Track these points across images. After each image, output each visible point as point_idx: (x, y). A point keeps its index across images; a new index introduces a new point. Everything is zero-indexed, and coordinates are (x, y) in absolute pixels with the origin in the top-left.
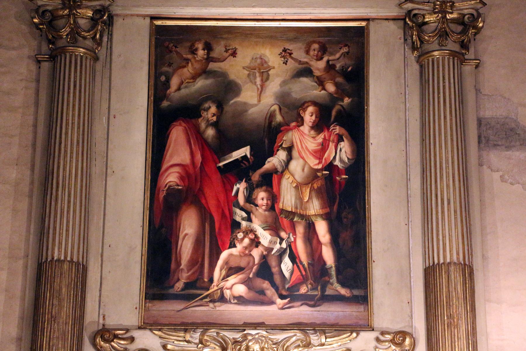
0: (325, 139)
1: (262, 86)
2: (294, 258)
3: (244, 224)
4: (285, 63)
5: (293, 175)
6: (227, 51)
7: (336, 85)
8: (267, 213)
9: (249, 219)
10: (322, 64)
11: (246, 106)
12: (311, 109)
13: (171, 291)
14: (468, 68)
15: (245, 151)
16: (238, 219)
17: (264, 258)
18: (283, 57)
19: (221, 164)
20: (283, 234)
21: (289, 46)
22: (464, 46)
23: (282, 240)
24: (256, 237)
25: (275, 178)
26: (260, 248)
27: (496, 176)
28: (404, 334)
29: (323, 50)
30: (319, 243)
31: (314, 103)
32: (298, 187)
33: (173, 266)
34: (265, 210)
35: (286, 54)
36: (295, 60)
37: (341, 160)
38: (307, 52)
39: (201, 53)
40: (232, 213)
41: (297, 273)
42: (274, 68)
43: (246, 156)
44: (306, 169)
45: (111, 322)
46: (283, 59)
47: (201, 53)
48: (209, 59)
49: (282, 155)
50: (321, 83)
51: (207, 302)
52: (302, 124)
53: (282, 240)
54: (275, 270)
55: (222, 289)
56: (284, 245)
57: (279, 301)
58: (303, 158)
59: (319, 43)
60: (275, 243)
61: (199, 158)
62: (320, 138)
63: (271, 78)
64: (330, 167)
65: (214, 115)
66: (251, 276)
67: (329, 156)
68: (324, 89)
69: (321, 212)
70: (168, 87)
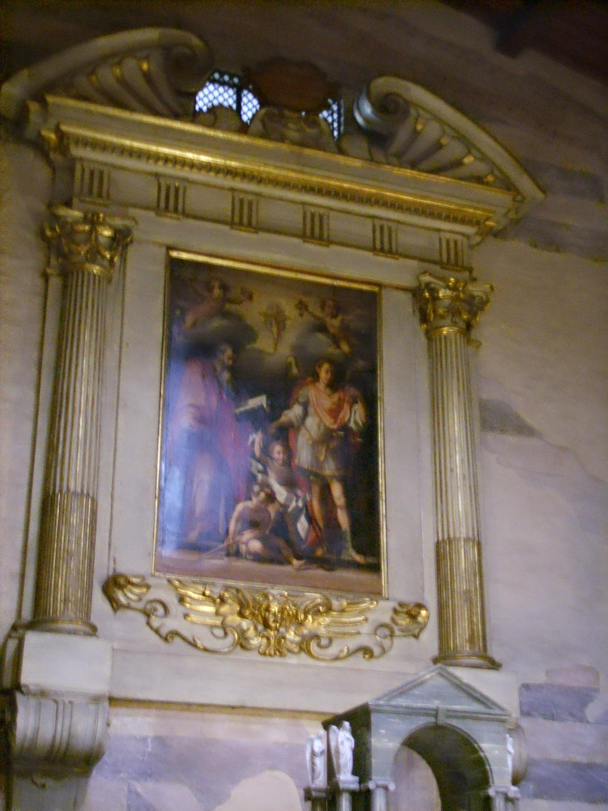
0: (340, 399)
1: (279, 334)
2: (311, 519)
3: (260, 477)
7: (351, 346)
8: (283, 468)
9: (265, 472)
10: (336, 322)
12: (326, 366)
16: (254, 471)
18: (301, 309)
20: (299, 492)
21: (306, 299)
26: (276, 505)
32: (315, 444)
35: (302, 307)
36: (311, 314)
37: (355, 422)
38: (323, 307)
39: (217, 292)
41: (313, 535)
42: (290, 318)
43: (262, 406)
44: (322, 428)
45: (124, 567)
47: (217, 292)
49: (297, 410)
50: (336, 342)
53: (298, 497)
56: (300, 504)
57: (295, 562)
58: (319, 416)
59: (334, 301)
60: (291, 501)
62: (336, 397)
64: (345, 427)
66: (267, 532)
67: (344, 417)
68: (338, 347)
69: (336, 473)
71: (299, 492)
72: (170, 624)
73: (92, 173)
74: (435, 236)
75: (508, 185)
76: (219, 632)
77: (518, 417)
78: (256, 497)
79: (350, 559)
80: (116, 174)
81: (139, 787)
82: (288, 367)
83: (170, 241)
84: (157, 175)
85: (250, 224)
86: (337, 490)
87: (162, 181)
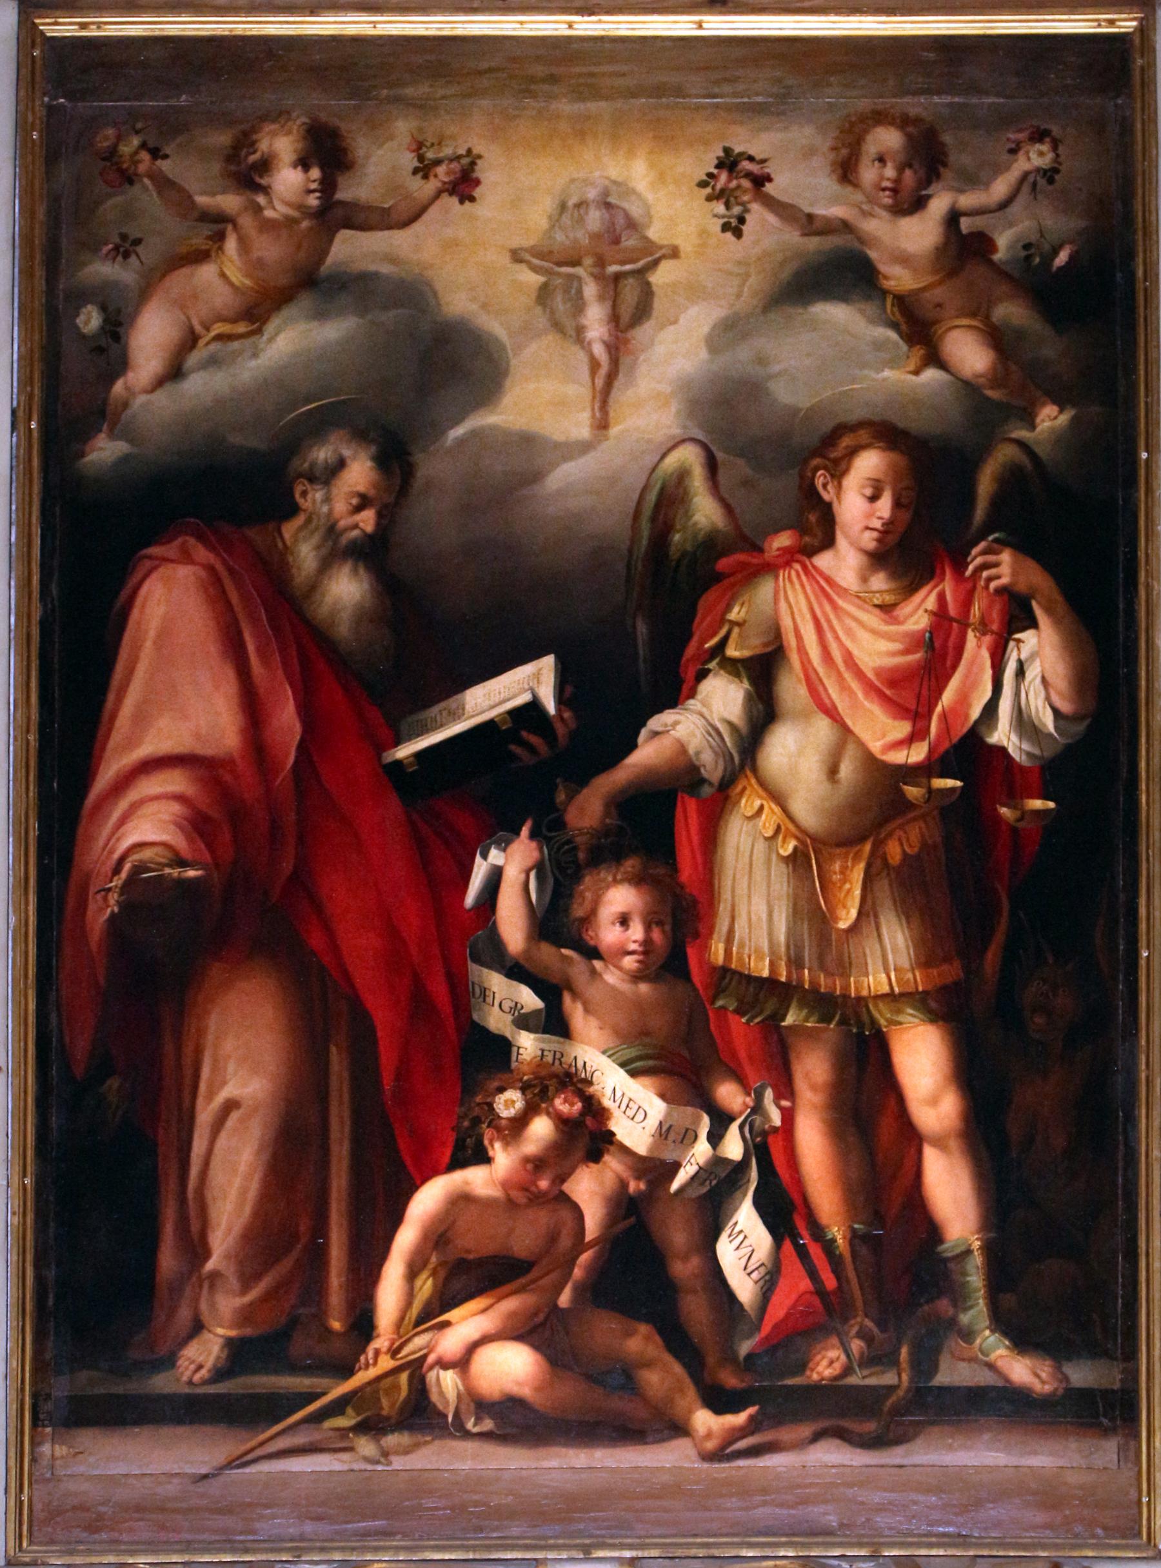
0: (940, 615)
1: (617, 348)
3: (528, 1044)
4: (735, 228)
5: (778, 798)
6: (424, 170)
8: (644, 988)
13: (161, 1383)
16: (497, 1021)
19: (404, 751)
20: (729, 1094)
23: (721, 1121)
24: (595, 1111)
26: (613, 1164)
33: (168, 1260)
34: (636, 977)
37: (1023, 723)
38: (846, 171)
42: (674, 253)
43: (534, 706)
44: (847, 770)
46: (720, 208)
51: (343, 1432)
52: (828, 542)
53: (721, 1121)
54: (684, 1269)
55: (417, 1368)
56: (733, 1148)
57: (704, 1420)
58: (831, 712)
60: (688, 1137)
63: (658, 304)
65: (364, 502)
66: (565, 1299)
67: (964, 699)
68: (934, 358)
69: (918, 980)
70: (121, 364)
71: (729, 1094)
78: (506, 1144)
79: (984, 1378)
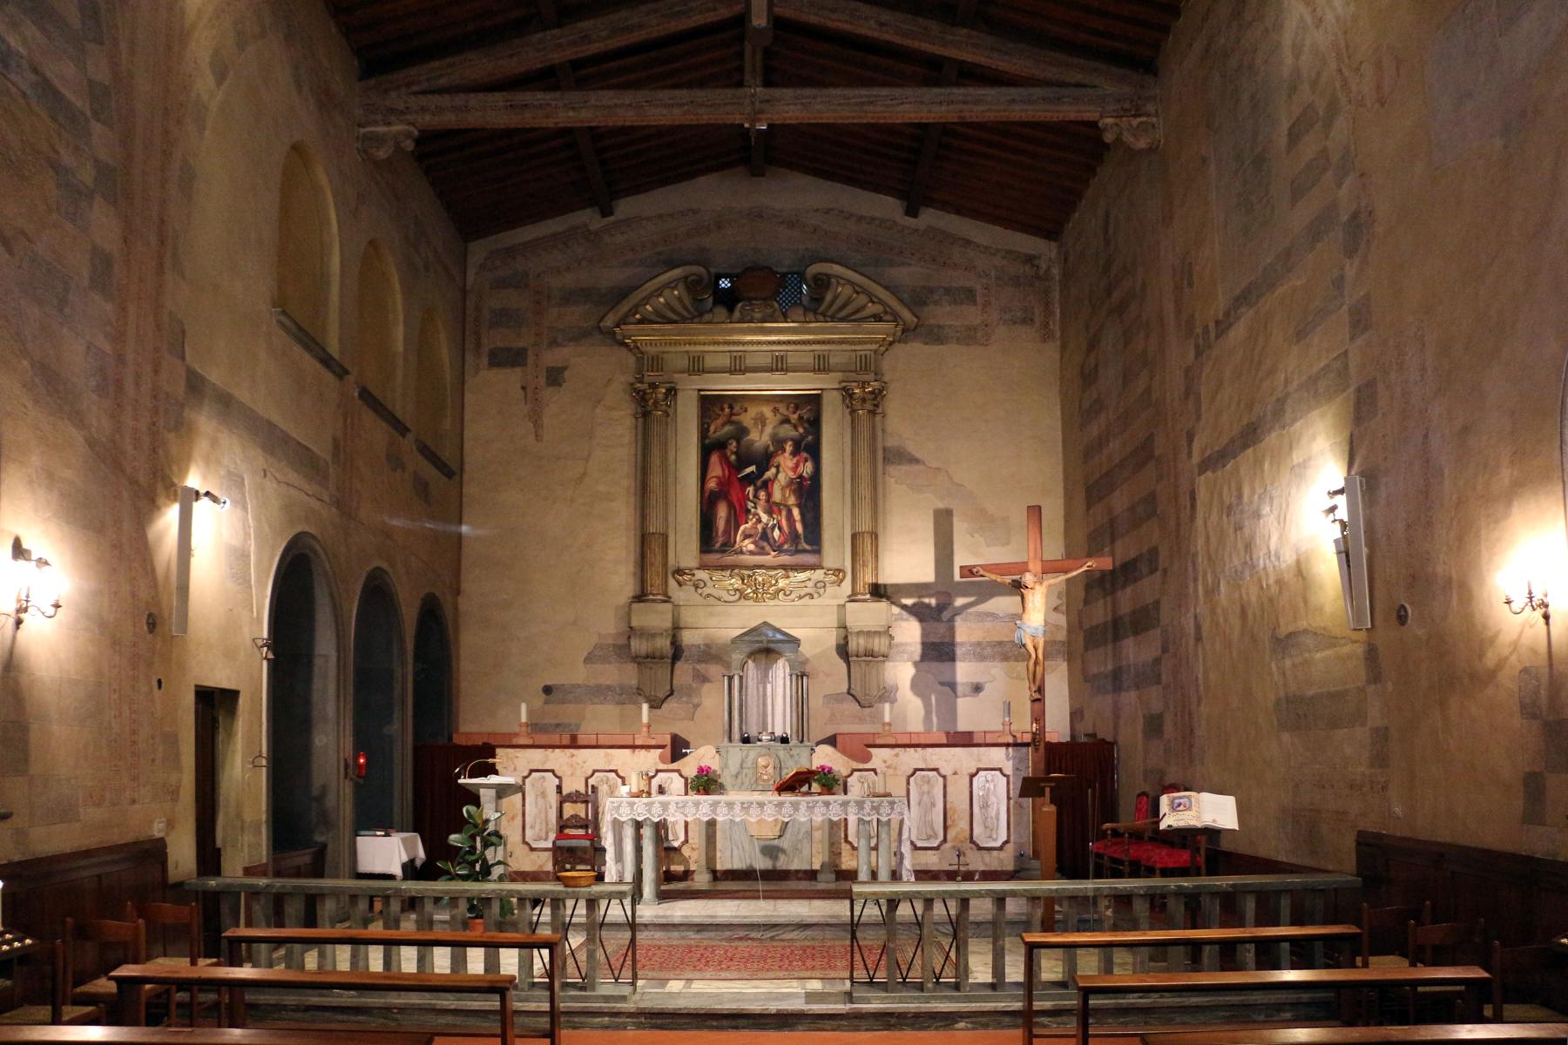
2: (780, 529)
3: (753, 510)
7: (804, 428)
9: (756, 508)
10: (796, 416)
11: (752, 442)
12: (790, 443)
14: (878, 418)
15: (752, 468)
17: (764, 529)
20: (775, 516)
22: (876, 406)
25: (770, 484)
27: (893, 480)
28: (839, 570)
29: (797, 408)
30: (795, 521)
31: (792, 440)
32: (783, 489)
33: (714, 534)
35: (775, 410)
38: (788, 409)
39: (727, 410)
40: (746, 505)
41: (782, 538)
45: (683, 565)
47: (727, 410)
48: (732, 414)
49: (773, 470)
50: (795, 427)
54: (770, 536)
57: (773, 553)
61: (727, 472)
62: (795, 460)
64: (801, 477)
71: (775, 516)
72: (707, 591)
73: (653, 358)
74: (853, 354)
75: (896, 318)
76: (732, 593)
77: (909, 453)
80: (665, 356)
81: (698, 667)
82: (768, 447)
83: (699, 387)
84: (687, 352)
85: (740, 370)
86: (796, 512)
87: (691, 355)
